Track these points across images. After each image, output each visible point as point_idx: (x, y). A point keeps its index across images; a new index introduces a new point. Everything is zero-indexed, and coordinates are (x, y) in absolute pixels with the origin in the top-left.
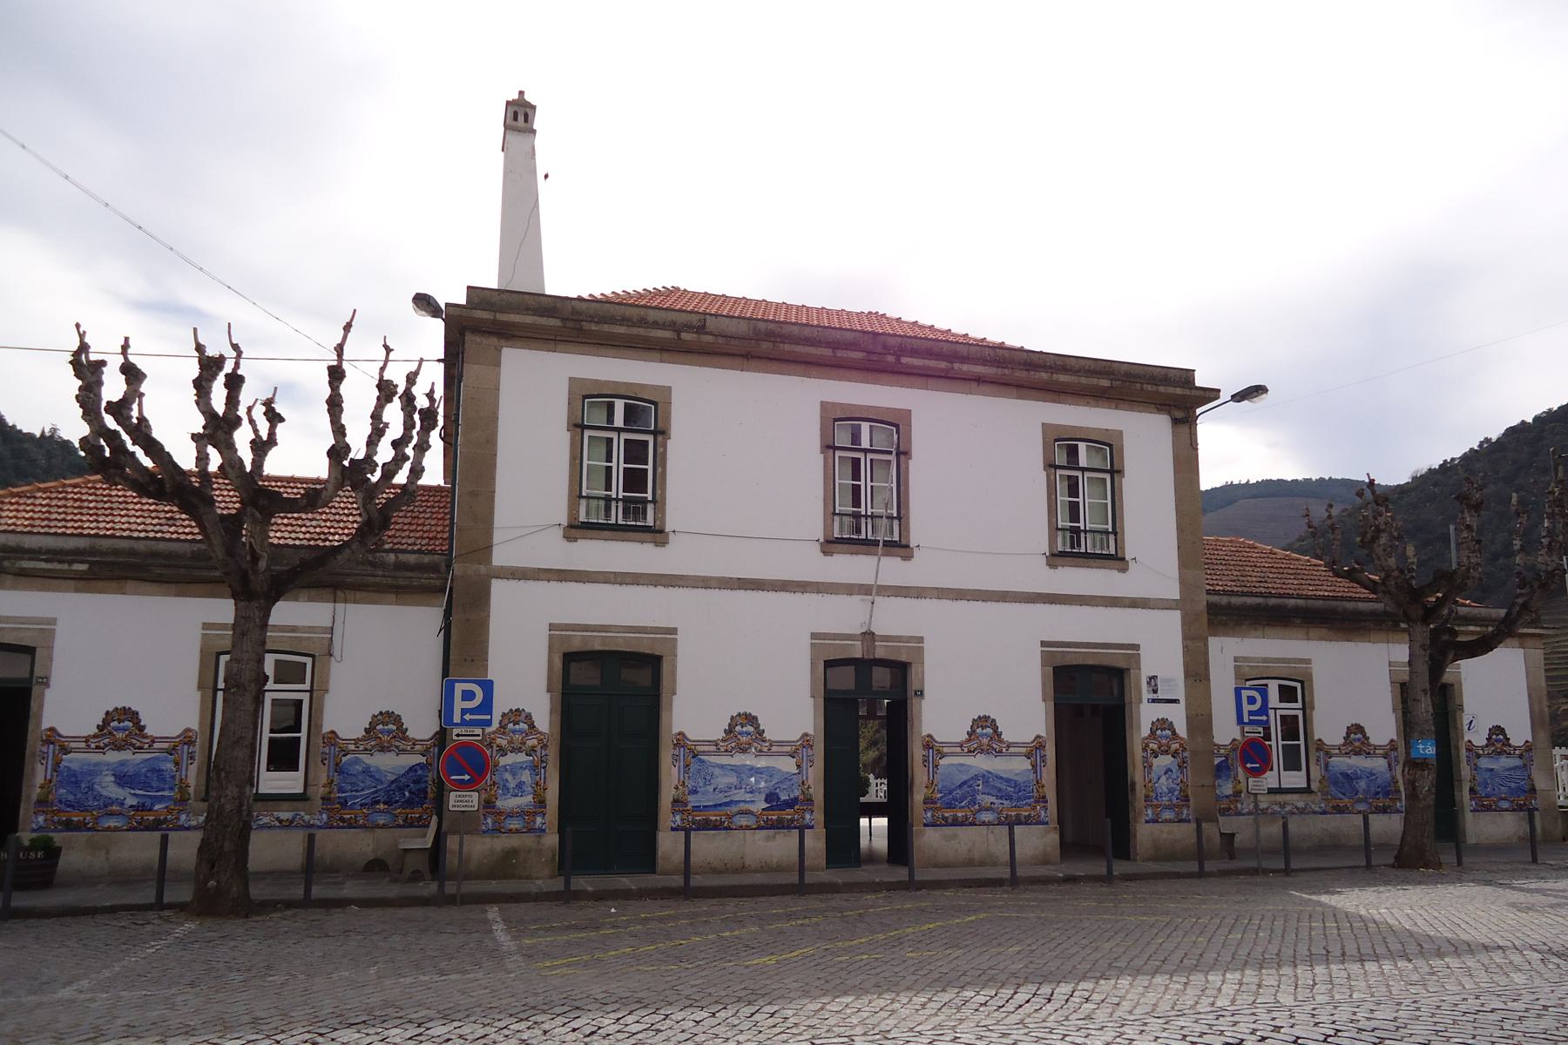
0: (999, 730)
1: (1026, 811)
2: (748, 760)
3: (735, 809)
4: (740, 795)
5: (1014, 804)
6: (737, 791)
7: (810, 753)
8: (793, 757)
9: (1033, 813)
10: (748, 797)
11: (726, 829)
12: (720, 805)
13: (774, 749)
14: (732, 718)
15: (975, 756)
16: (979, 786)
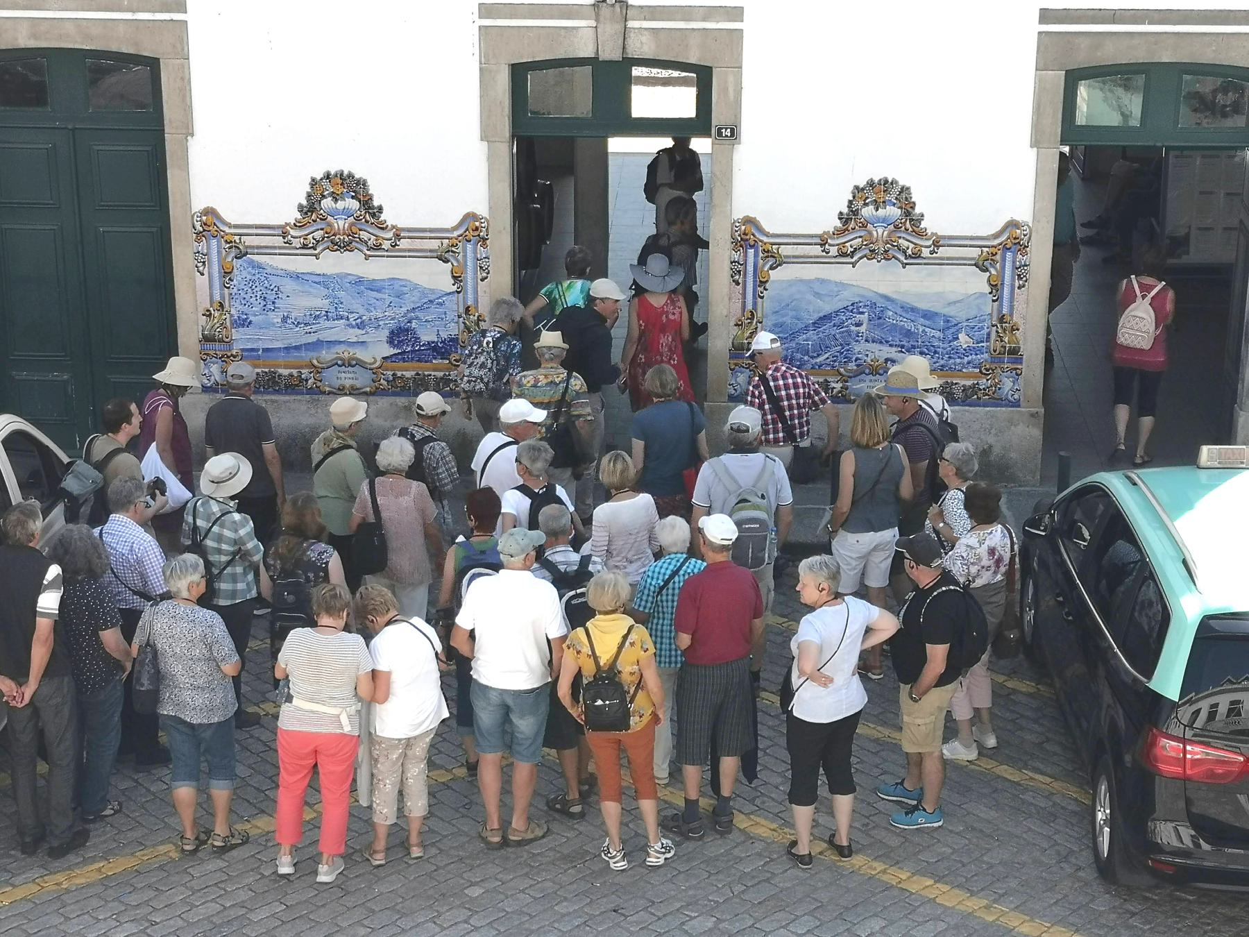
0: (918, 210)
1: (968, 376)
2: (351, 264)
3: (327, 355)
4: (335, 331)
5: (942, 362)
6: (328, 324)
7: (481, 252)
8: (446, 261)
9: (983, 383)
10: (353, 335)
11: (310, 391)
12: (297, 348)
13: (404, 244)
14: (314, 183)
15: (854, 264)
16: (859, 325)
